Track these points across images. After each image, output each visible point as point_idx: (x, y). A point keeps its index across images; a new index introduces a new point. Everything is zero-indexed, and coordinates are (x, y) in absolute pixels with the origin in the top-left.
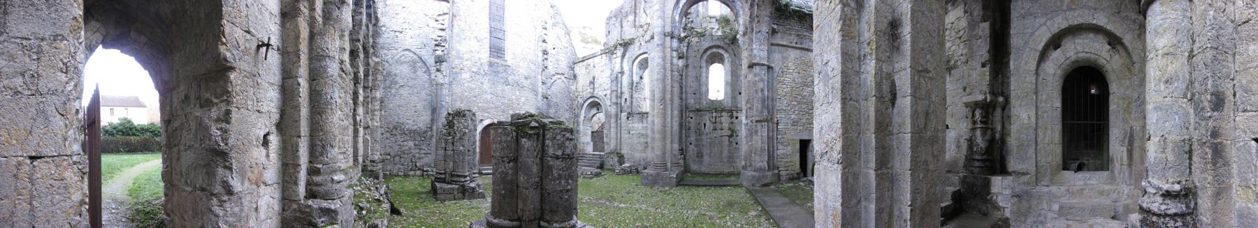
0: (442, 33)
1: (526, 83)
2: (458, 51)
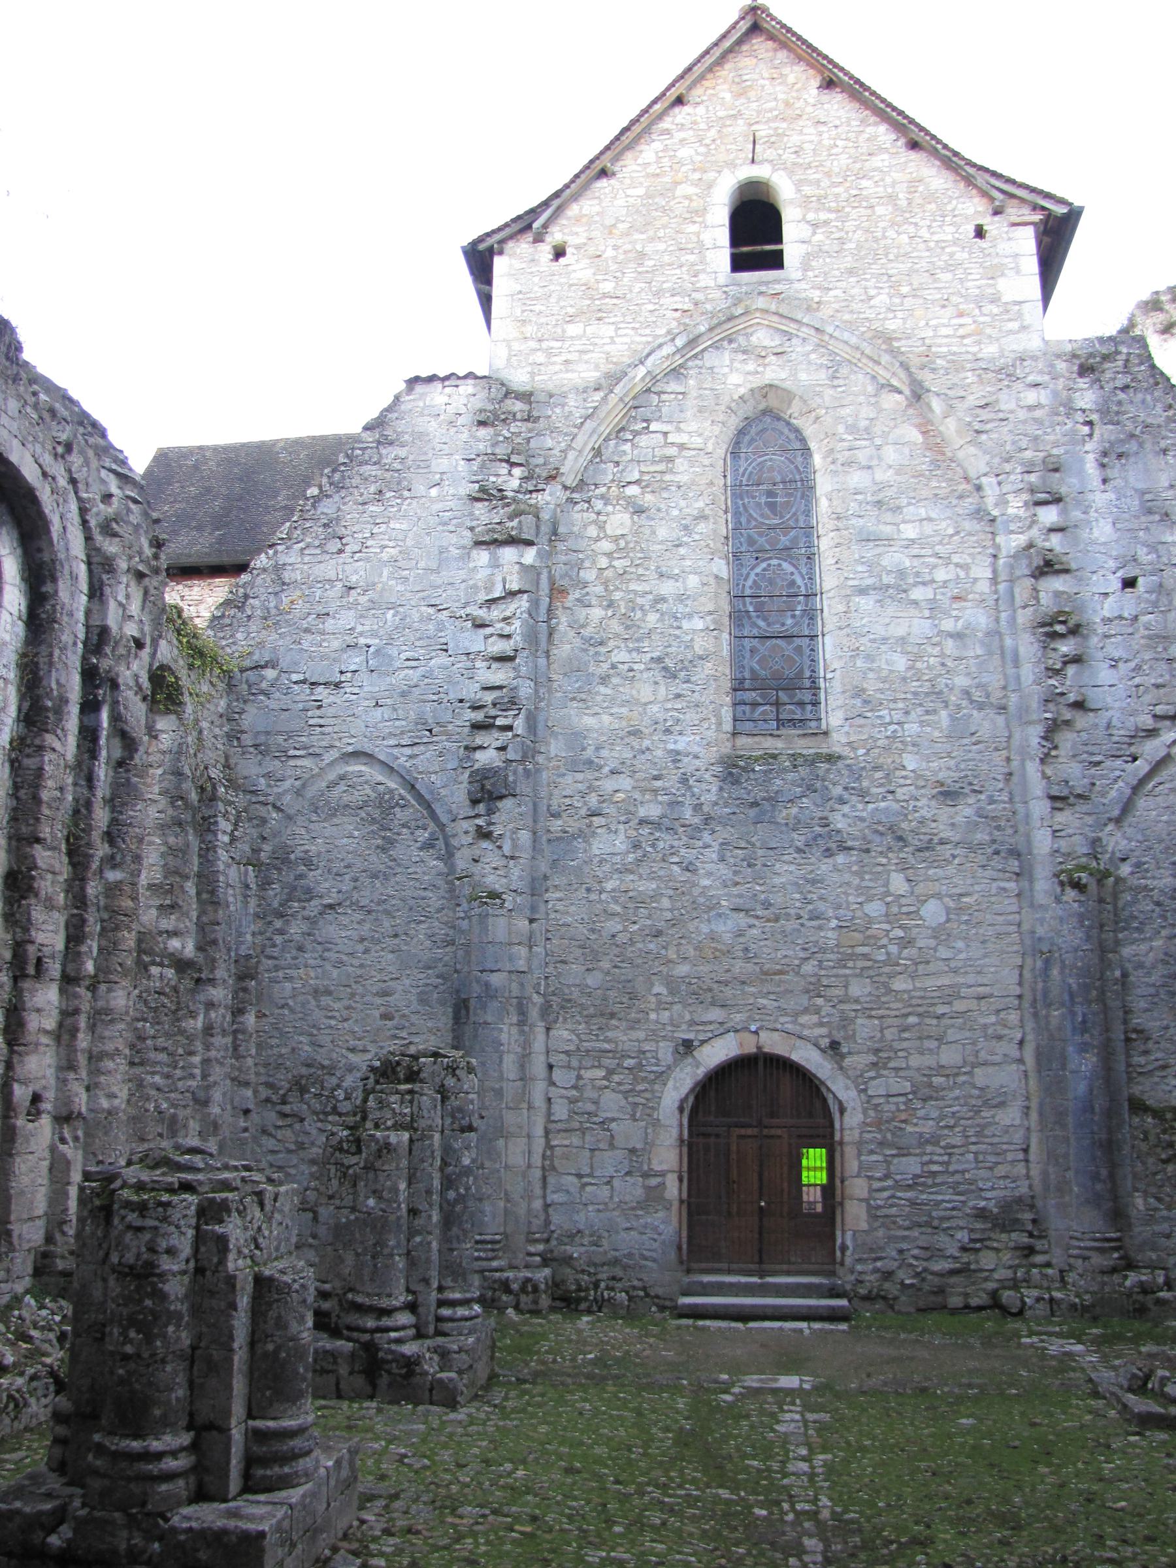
0: (499, 675)
1: (947, 821)
2: (577, 738)
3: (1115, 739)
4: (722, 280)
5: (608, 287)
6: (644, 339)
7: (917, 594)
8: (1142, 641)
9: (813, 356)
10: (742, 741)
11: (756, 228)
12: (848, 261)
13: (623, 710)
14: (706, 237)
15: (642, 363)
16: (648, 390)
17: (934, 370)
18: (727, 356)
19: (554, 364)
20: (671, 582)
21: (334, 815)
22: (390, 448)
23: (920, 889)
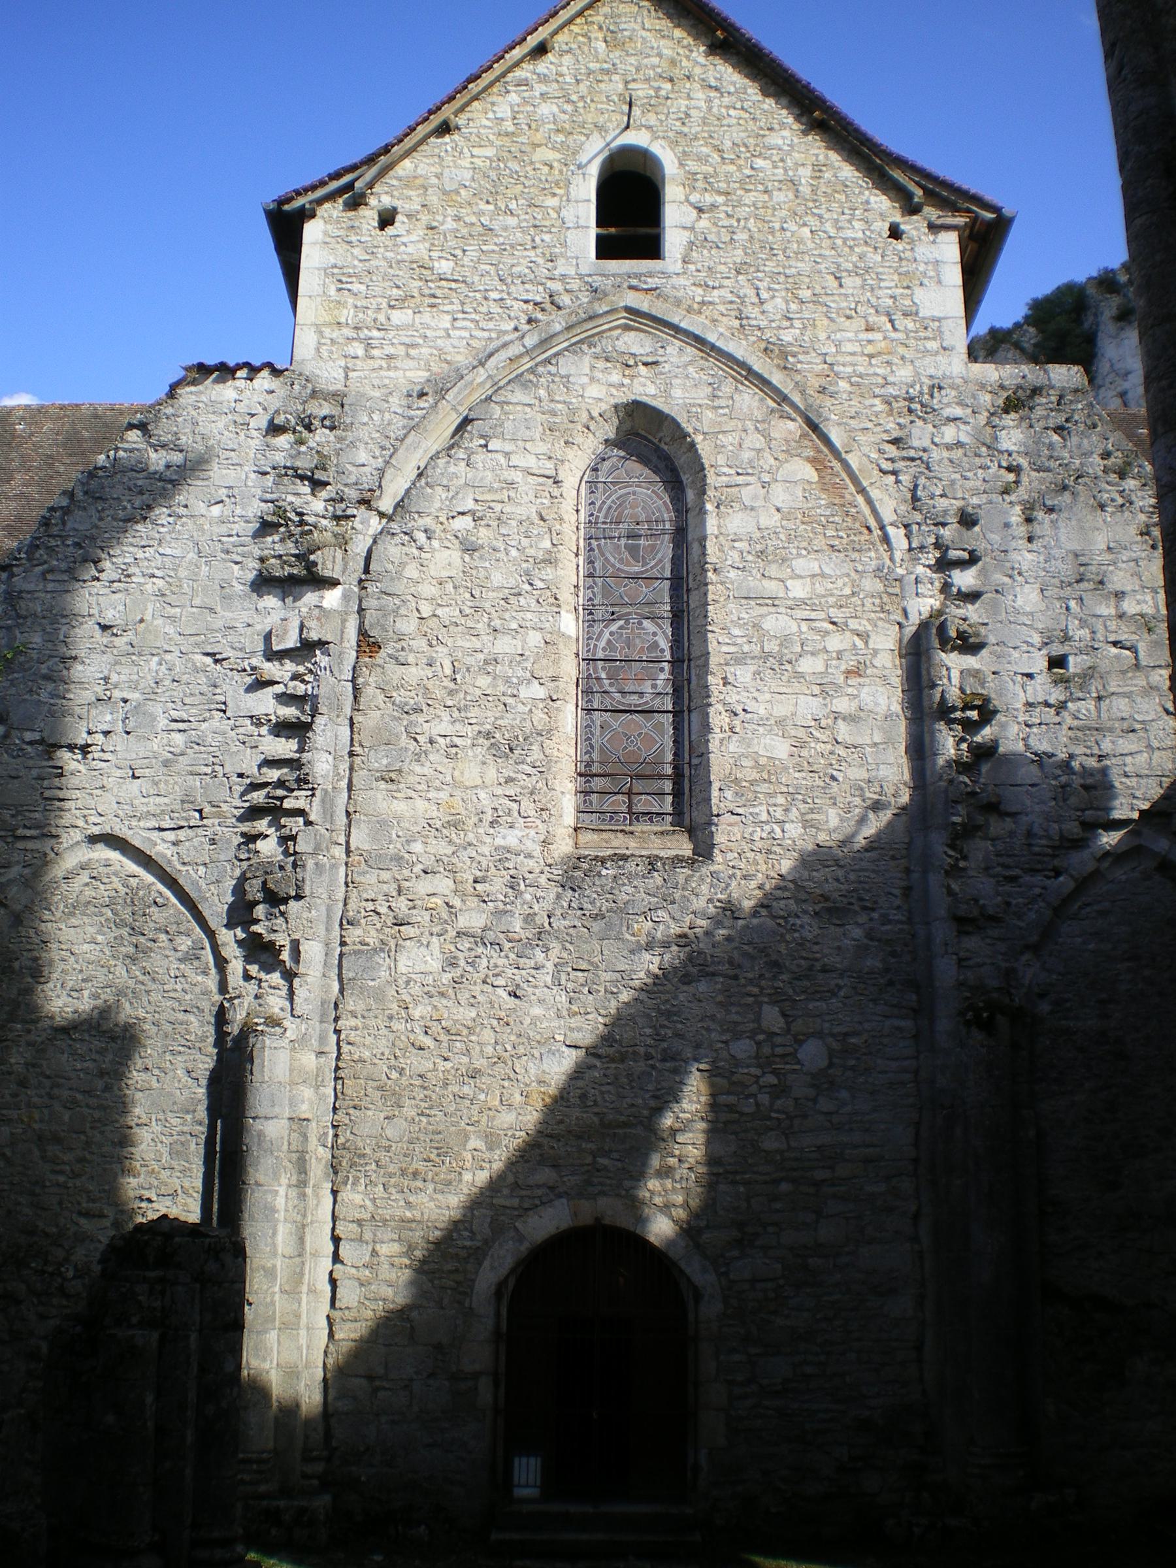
3: (1037, 849)
4: (584, 270)
5: (444, 266)
6: (486, 334)
7: (808, 665)
8: (1070, 733)
9: (691, 369)
10: (586, 837)
11: (630, 207)
12: (738, 255)
13: (443, 795)
14: (568, 214)
18: (587, 360)
20: (507, 639)
21: (73, 914)
22: (162, 453)
23: (798, 1025)
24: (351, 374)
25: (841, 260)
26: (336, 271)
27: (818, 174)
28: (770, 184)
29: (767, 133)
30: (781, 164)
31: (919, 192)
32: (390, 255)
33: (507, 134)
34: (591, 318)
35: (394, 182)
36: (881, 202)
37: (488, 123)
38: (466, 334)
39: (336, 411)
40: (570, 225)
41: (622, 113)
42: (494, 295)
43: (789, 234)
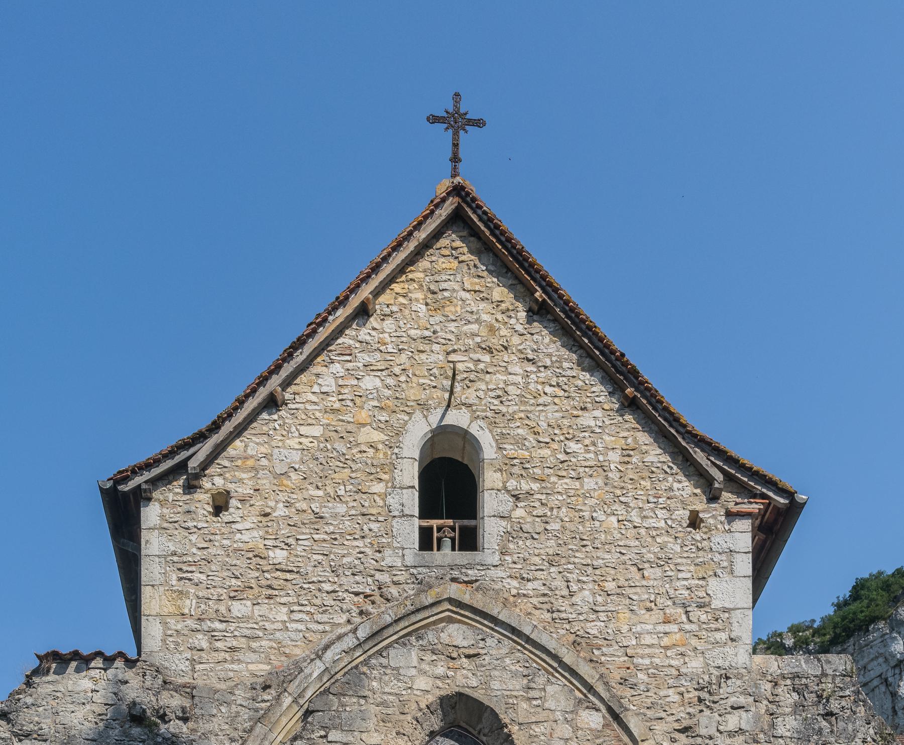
4: (410, 560)
5: (279, 555)
6: (321, 627)
9: (508, 661)
11: (449, 487)
12: (551, 546)
15: (319, 657)
16: (327, 691)
17: (633, 687)
18: (414, 655)
19: (216, 650)
24: (198, 667)
25: (644, 551)
26: (175, 559)
27: (626, 459)
28: (581, 470)
29: (580, 413)
30: (592, 448)
31: (718, 476)
32: (225, 542)
33: (334, 411)
34: (418, 610)
35: (226, 463)
36: (685, 488)
37: (314, 398)
38: (301, 627)
39: (187, 703)
40: (396, 513)
41: (443, 389)
42: (327, 587)
43: (597, 524)
